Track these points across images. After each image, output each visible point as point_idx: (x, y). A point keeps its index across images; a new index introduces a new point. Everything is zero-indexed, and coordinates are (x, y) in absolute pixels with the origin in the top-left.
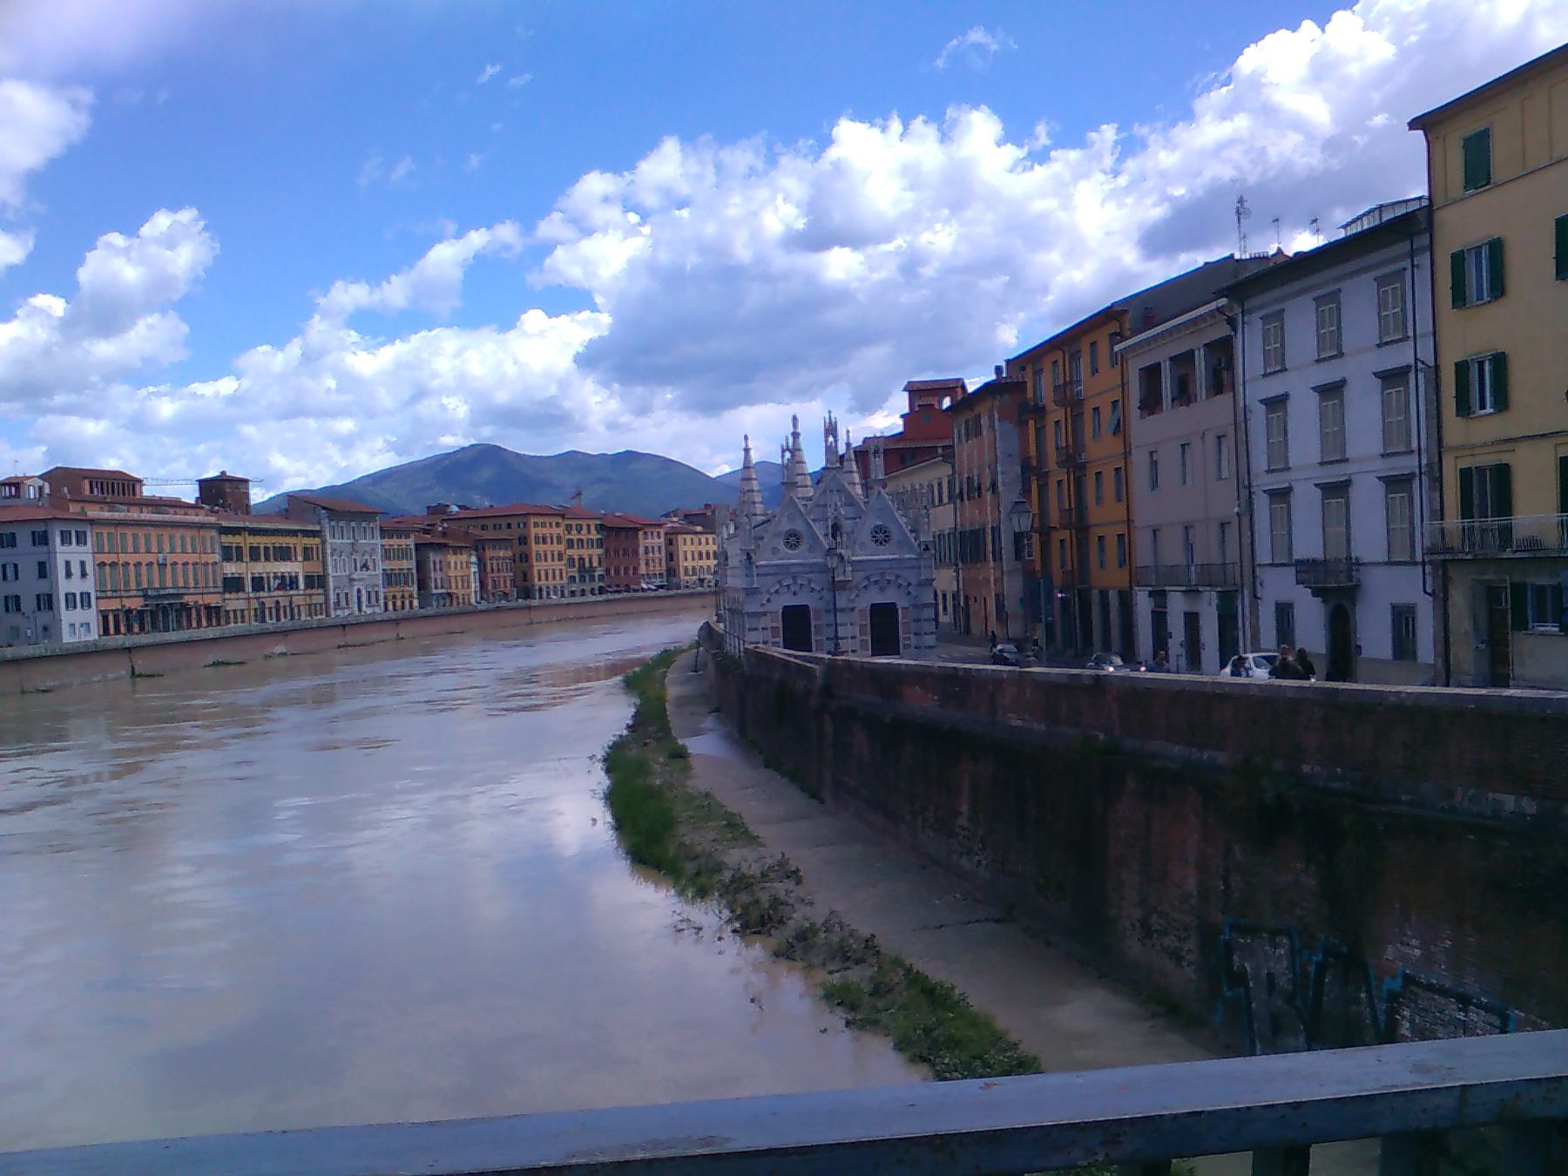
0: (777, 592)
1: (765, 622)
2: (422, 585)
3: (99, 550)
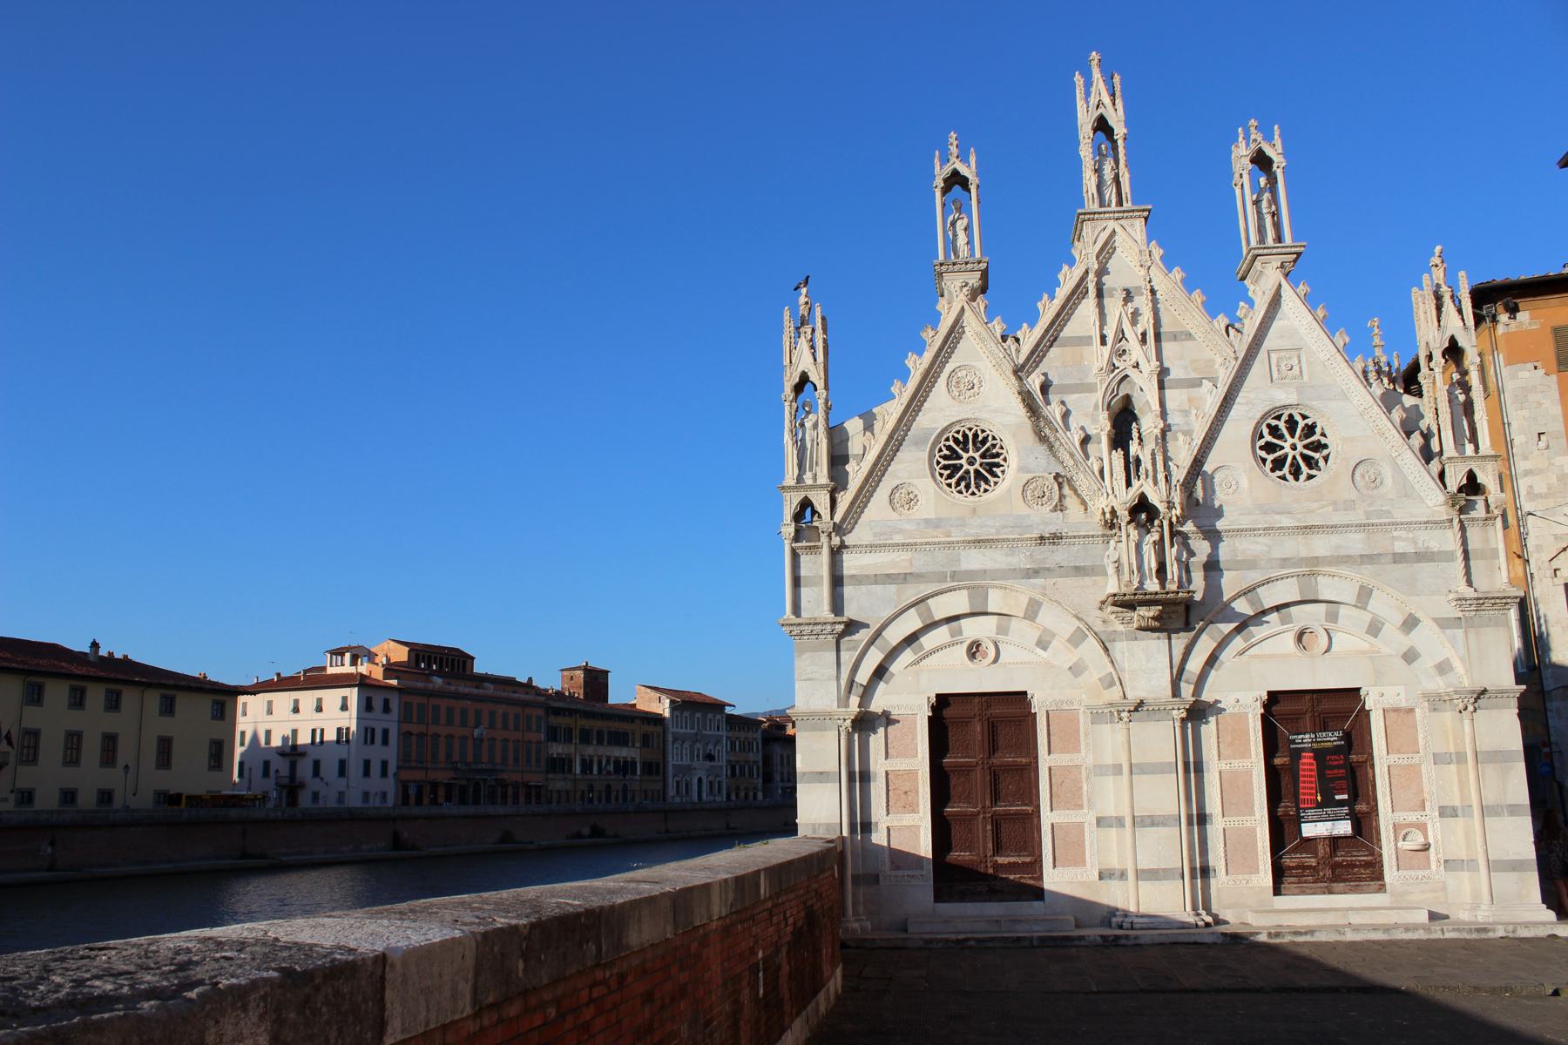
3: (406, 717)
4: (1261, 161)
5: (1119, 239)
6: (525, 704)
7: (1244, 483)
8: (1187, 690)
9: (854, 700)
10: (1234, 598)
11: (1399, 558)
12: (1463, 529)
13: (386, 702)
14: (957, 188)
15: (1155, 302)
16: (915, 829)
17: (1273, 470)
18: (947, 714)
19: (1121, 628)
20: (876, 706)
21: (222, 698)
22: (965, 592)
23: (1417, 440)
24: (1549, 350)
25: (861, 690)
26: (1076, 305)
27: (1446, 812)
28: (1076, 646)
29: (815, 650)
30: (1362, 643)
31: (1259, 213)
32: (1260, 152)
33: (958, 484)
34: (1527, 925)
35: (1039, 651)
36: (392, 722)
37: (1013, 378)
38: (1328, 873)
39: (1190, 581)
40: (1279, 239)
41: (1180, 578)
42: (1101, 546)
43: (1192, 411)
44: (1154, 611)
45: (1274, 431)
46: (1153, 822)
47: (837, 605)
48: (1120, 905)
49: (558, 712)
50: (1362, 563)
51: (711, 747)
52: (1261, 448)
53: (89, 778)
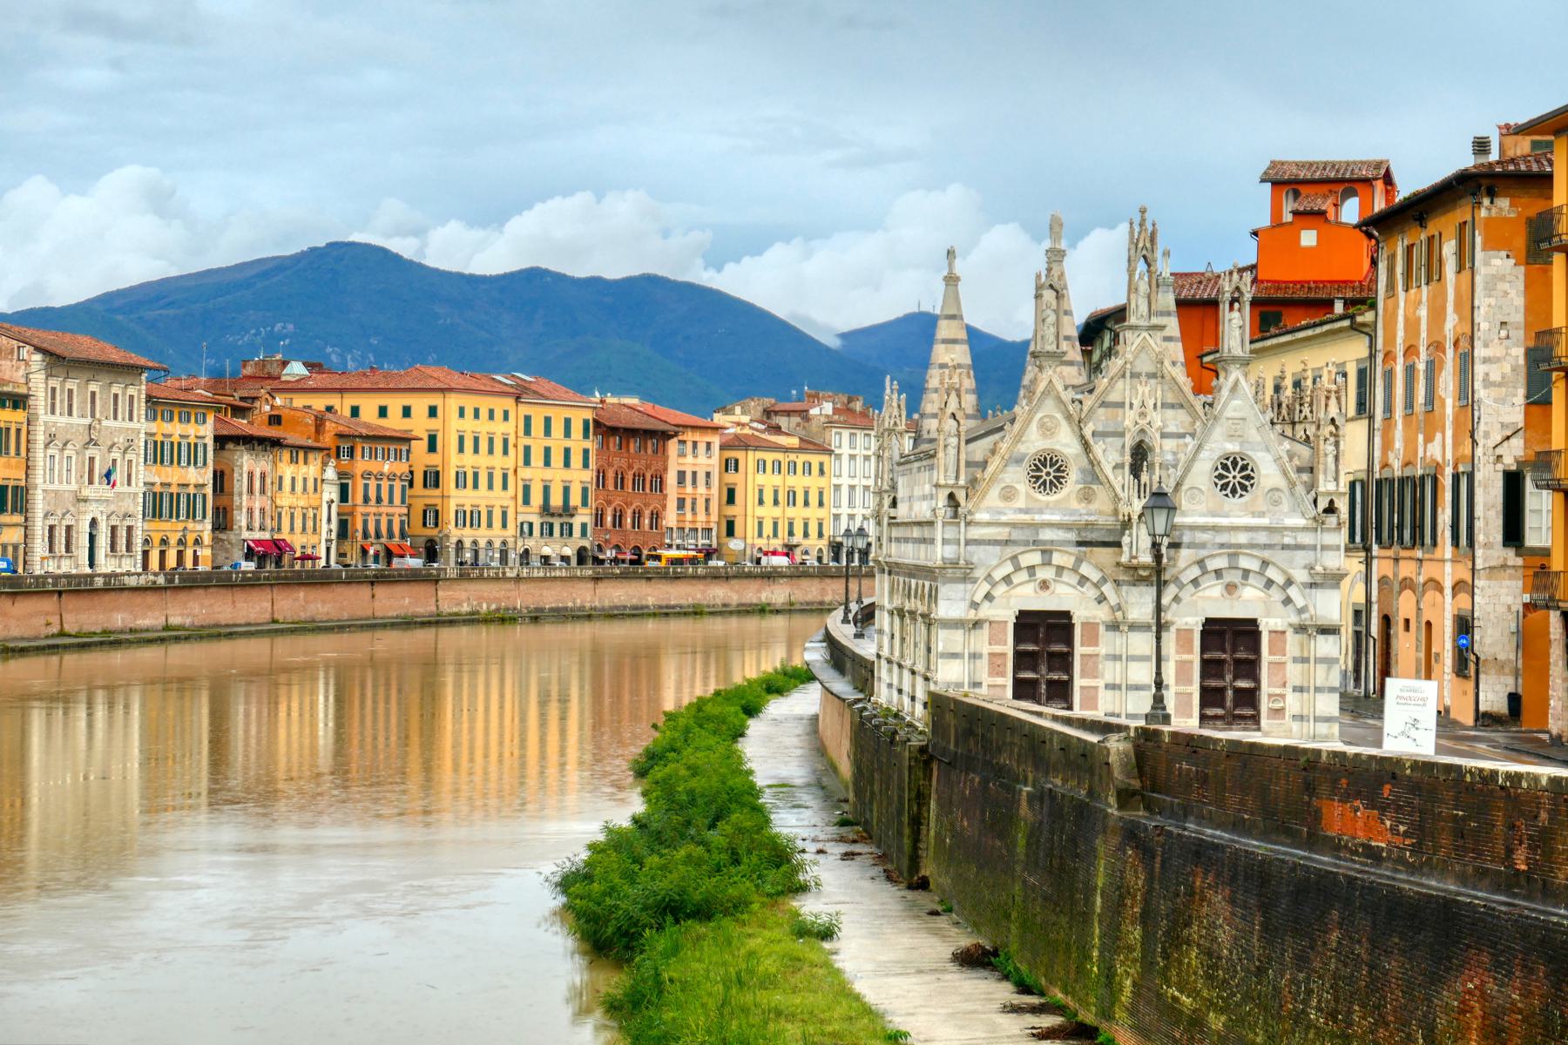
0: (1007, 579)
1: (981, 642)
2: (222, 521)
11: (1284, 547)
24: (1520, 242)
27: (1295, 689)
45: (1225, 467)
46: (1137, 688)
51: (116, 454)
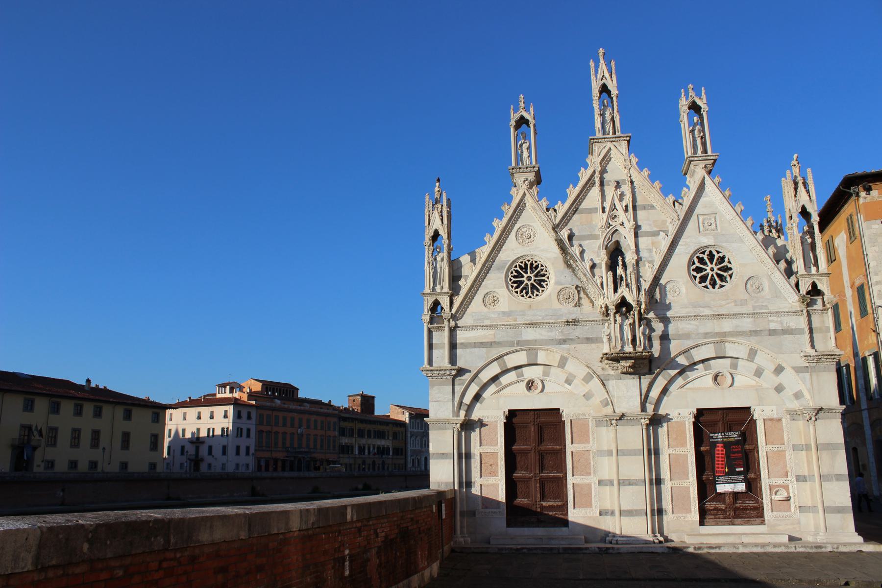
3: (260, 422)
4: (695, 108)
5: (614, 152)
6: (327, 415)
7: (684, 290)
8: (650, 408)
9: (462, 413)
10: (677, 356)
11: (772, 332)
12: (809, 315)
13: (249, 413)
14: (524, 126)
15: (633, 189)
16: (496, 486)
17: (700, 283)
18: (514, 421)
19: (612, 372)
20: (475, 416)
21: (158, 411)
22: (525, 352)
23: (783, 265)
25: (466, 407)
26: (588, 191)
27: (800, 479)
28: (587, 383)
29: (441, 384)
30: (752, 381)
31: (694, 137)
32: (694, 103)
33: (521, 292)
34: (845, 544)
35: (566, 385)
36: (252, 425)
37: (552, 232)
38: (732, 513)
39: (651, 346)
40: (705, 151)
41: (645, 344)
42: (601, 326)
43: (653, 250)
44: (629, 363)
45: (701, 260)
46: (630, 483)
47: (453, 360)
48: (611, 531)
49: (345, 419)
50: (751, 335)
52: (693, 270)
53: (84, 455)
